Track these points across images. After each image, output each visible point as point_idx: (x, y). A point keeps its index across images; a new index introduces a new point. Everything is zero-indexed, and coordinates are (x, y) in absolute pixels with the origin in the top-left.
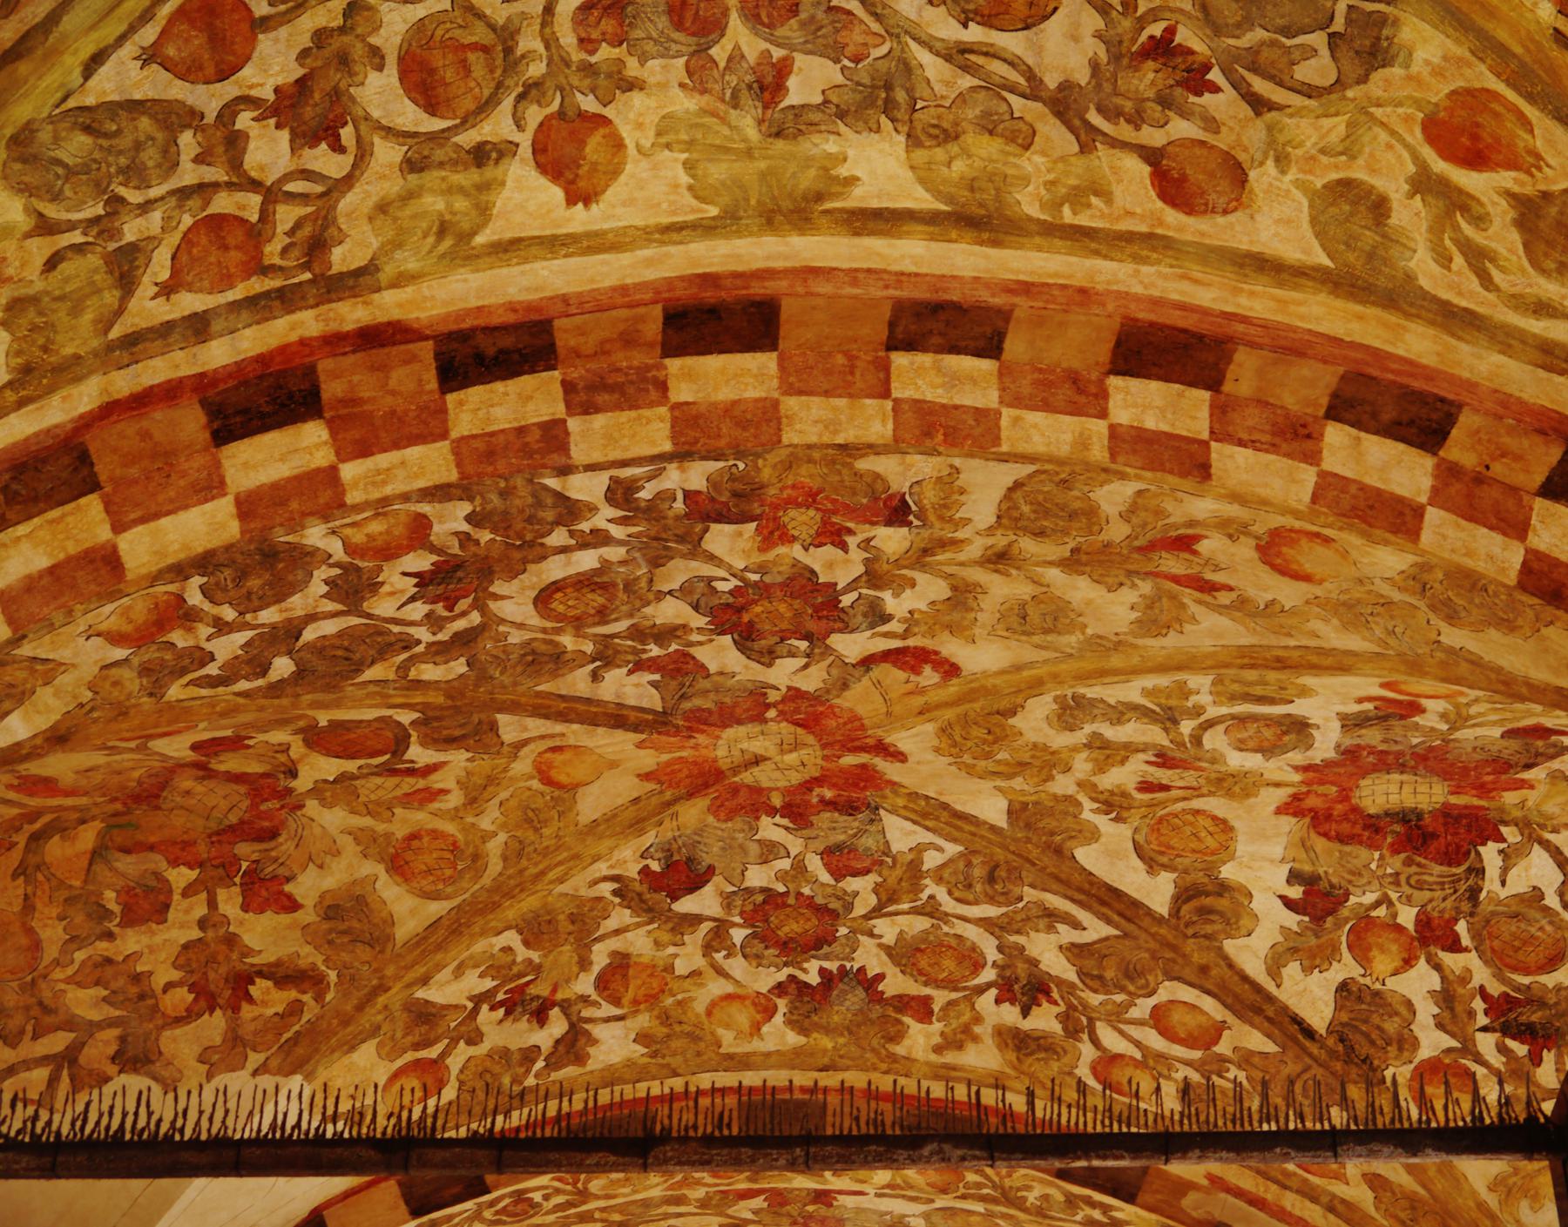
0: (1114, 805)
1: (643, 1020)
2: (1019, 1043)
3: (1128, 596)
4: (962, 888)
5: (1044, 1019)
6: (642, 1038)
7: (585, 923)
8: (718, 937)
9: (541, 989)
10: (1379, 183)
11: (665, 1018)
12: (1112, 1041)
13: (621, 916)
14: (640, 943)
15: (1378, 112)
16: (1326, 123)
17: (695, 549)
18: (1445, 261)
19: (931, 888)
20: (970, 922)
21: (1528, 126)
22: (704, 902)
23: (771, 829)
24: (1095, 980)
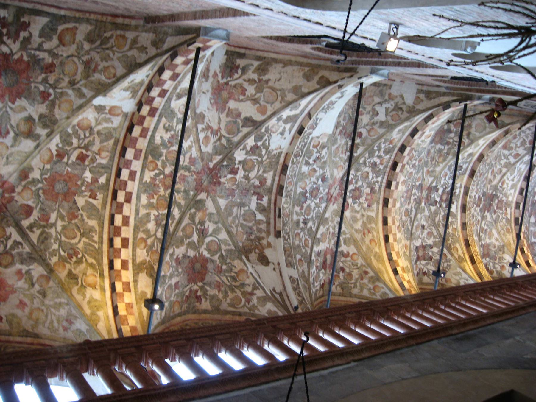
0: (328, 229)
1: (307, 173)
2: (298, 222)
3: (360, 228)
4: (317, 213)
5: (302, 225)
6: (304, 172)
7: (323, 168)
8: (314, 183)
9: (318, 162)
11: (306, 176)
12: (302, 234)
13: (322, 172)
14: (318, 174)
17: (367, 187)
19: (317, 209)
20: (313, 214)
22: (320, 182)
23: (327, 190)
24: (308, 230)
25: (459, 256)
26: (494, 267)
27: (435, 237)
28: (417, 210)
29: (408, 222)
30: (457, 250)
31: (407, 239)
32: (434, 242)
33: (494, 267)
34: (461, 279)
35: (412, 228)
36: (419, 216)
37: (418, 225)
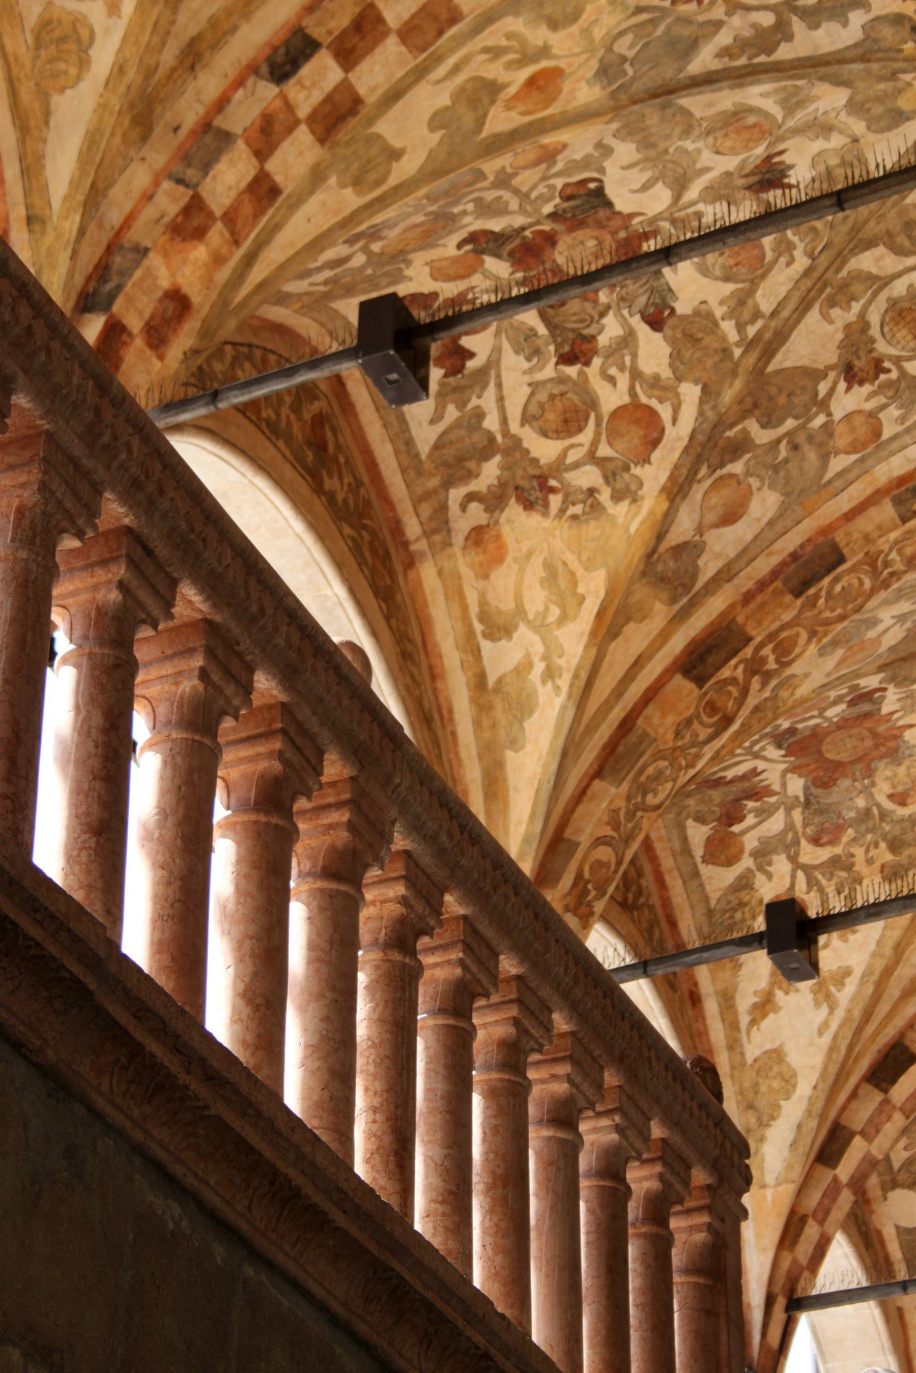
10: (562, 34)
15: (585, 56)
16: (604, 31)
18: (509, 36)
21: (523, 114)
25: (689, 550)
26: (763, 854)
27: (740, 304)
28: (864, 52)
29: (738, 25)
30: (729, 518)
31: (605, 72)
32: (704, 317)
33: (763, 854)
34: (540, 627)
35: (708, 80)
36: (830, 99)
37: (764, 128)
